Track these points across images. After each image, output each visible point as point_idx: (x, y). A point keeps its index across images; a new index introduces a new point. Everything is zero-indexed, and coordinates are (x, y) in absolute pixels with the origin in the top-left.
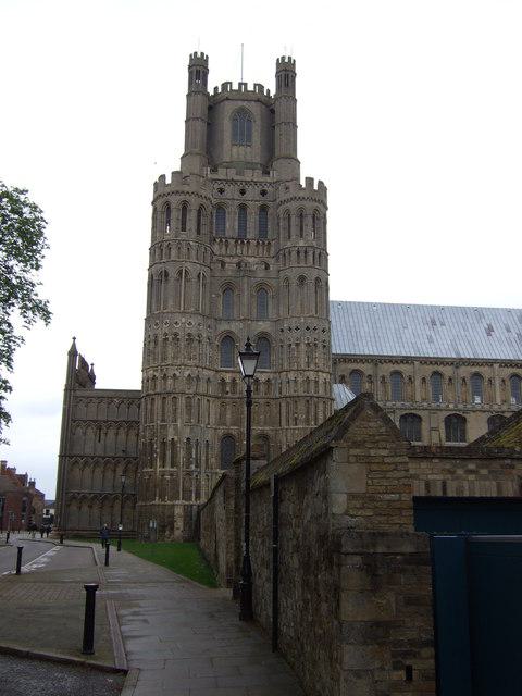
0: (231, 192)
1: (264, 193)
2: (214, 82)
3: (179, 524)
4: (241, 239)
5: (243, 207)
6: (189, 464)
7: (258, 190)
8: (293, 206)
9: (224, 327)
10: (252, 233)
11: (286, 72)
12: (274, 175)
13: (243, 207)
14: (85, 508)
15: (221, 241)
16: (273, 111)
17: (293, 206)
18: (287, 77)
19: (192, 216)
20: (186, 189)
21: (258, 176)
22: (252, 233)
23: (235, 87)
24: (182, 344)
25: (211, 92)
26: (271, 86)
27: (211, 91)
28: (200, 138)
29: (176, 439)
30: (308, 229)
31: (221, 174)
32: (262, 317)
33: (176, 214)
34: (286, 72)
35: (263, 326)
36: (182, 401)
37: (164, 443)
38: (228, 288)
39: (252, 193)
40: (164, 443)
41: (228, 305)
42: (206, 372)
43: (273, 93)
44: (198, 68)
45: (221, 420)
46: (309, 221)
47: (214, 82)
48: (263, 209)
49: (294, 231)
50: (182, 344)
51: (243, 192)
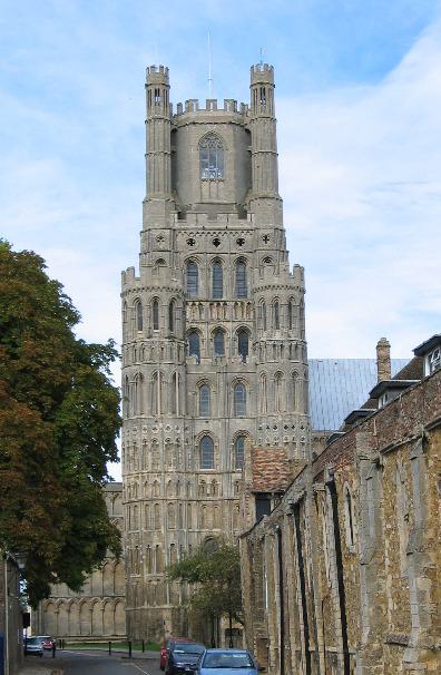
2: (177, 96)
3: (168, 627)
4: (216, 301)
5: (217, 261)
7: (234, 238)
8: (268, 295)
9: (200, 427)
10: (228, 294)
12: (252, 221)
14: (63, 614)
15: (194, 304)
16: (248, 131)
17: (268, 295)
19: (163, 312)
22: (228, 294)
26: (245, 97)
28: (164, 178)
29: (160, 544)
30: (283, 321)
31: (191, 222)
32: (239, 412)
33: (146, 313)
35: (239, 424)
38: (203, 384)
39: (227, 243)
41: (205, 400)
43: (248, 101)
46: (283, 311)
49: (270, 322)
51: (216, 243)
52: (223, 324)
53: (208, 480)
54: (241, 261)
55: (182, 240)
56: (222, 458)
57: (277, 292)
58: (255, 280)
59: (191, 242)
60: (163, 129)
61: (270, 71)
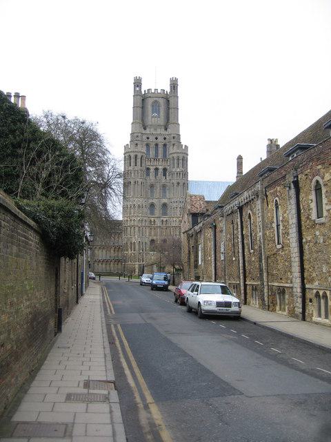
0: (152, 139)
1: (165, 139)
2: (144, 88)
3: (137, 270)
4: (156, 159)
5: (157, 145)
6: (139, 250)
8: (175, 155)
9: (150, 201)
10: (160, 156)
11: (174, 85)
13: (157, 145)
14: (100, 264)
17: (175, 155)
18: (174, 87)
19: (139, 160)
20: (136, 150)
21: (163, 131)
22: (160, 156)
23: (153, 91)
24: (136, 209)
25: (143, 93)
26: (168, 89)
27: (143, 93)
28: (139, 116)
30: (181, 165)
31: (148, 131)
32: (164, 197)
33: (133, 160)
34: (174, 85)
35: (165, 201)
36: (137, 229)
37: (131, 243)
38: (152, 186)
39: (160, 139)
40: (131, 243)
41: (152, 192)
42: (145, 218)
43: (169, 91)
44: (138, 83)
45: (150, 235)
47: (144, 88)
48: (165, 145)
49: (176, 165)
50: (136, 209)
51: (157, 139)
52: (158, 167)
53: (152, 219)
54: (165, 145)
55: (145, 137)
56: (158, 212)
57: (179, 155)
58: (171, 150)
59: (148, 138)
60: (139, 99)
61: (176, 80)
